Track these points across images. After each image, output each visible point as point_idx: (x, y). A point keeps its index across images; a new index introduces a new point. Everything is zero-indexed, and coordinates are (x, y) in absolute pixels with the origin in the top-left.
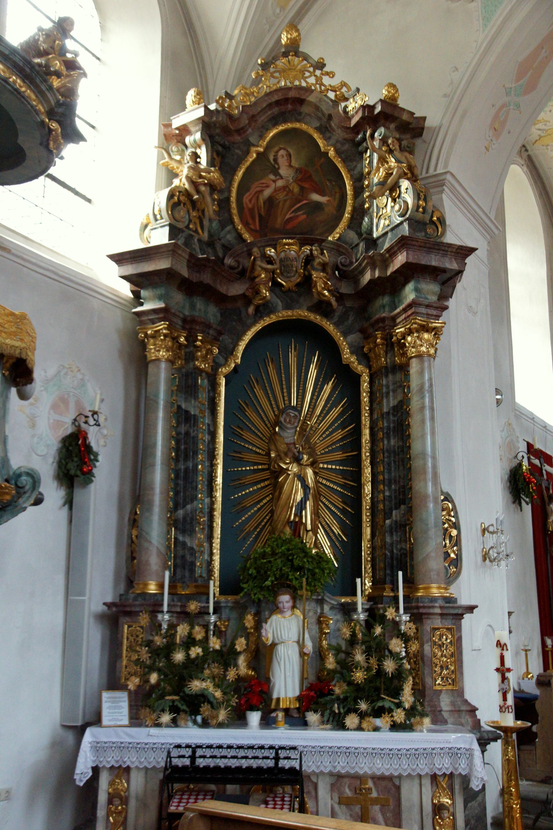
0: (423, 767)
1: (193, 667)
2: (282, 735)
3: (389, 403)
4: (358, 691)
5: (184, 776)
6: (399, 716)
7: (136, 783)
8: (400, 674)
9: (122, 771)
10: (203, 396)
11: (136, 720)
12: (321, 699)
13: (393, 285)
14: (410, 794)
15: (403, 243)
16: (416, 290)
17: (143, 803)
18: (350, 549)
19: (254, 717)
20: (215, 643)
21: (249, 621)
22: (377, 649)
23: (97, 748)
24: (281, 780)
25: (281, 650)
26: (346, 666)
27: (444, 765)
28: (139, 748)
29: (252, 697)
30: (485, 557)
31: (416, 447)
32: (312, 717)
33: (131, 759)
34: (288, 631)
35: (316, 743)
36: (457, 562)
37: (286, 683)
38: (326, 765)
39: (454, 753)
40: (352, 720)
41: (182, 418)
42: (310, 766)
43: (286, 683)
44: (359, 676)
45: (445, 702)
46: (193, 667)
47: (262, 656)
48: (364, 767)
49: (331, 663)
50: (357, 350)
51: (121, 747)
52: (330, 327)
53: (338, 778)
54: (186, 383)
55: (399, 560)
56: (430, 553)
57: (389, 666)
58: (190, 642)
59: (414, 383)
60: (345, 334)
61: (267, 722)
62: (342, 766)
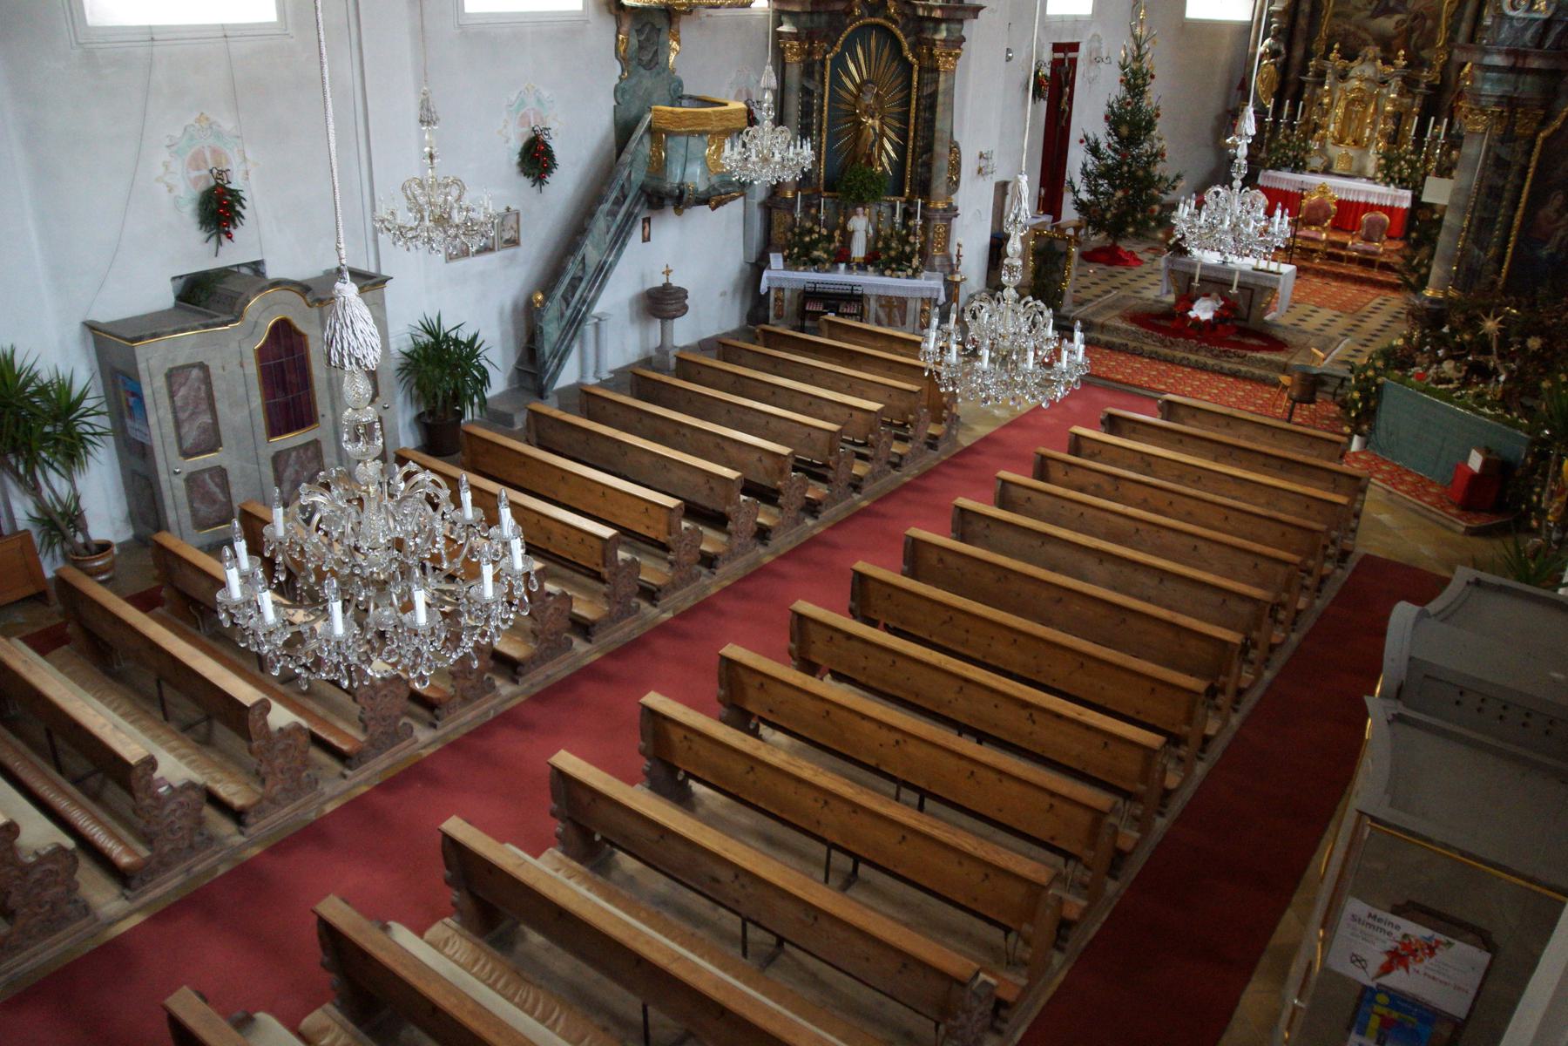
0: (918, 295)
1: (814, 244)
2: (856, 278)
3: (927, 91)
4: (892, 260)
5: (810, 295)
6: (910, 272)
7: (787, 294)
8: (913, 253)
9: (781, 289)
10: (817, 77)
11: (786, 268)
12: (875, 260)
13: (938, 21)
14: (911, 305)
15: (940, 7)
16: (948, 30)
17: (791, 303)
18: (899, 166)
19: (842, 266)
20: (824, 232)
21: (841, 219)
22: (904, 241)
23: (769, 279)
24: (852, 299)
25: (857, 235)
26: (887, 247)
27: (927, 294)
28: (788, 280)
29: (842, 256)
30: (980, 171)
31: (938, 125)
32: (870, 269)
33: (785, 285)
34: (860, 225)
35: (870, 281)
36: (957, 183)
37: (859, 250)
38: (875, 291)
39: (932, 289)
40: (888, 272)
41: (807, 92)
42: (866, 292)
43: (859, 250)
44: (893, 253)
45: (937, 262)
46: (814, 244)
47: (848, 236)
48: (891, 293)
49: (880, 244)
50: (913, 48)
51: (780, 279)
52: (898, 32)
53: (879, 297)
54: (808, 71)
55: (924, 188)
56: (939, 185)
57: (908, 249)
58: (811, 231)
59: (942, 86)
60: (906, 37)
61: (849, 268)
62: (881, 292)
